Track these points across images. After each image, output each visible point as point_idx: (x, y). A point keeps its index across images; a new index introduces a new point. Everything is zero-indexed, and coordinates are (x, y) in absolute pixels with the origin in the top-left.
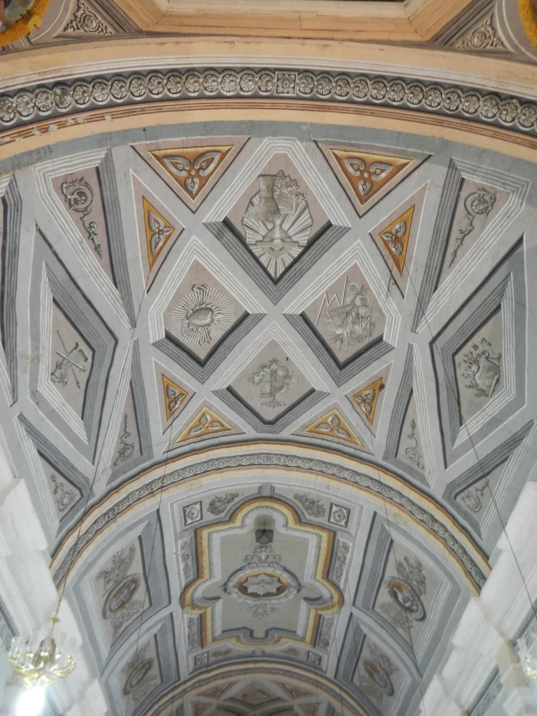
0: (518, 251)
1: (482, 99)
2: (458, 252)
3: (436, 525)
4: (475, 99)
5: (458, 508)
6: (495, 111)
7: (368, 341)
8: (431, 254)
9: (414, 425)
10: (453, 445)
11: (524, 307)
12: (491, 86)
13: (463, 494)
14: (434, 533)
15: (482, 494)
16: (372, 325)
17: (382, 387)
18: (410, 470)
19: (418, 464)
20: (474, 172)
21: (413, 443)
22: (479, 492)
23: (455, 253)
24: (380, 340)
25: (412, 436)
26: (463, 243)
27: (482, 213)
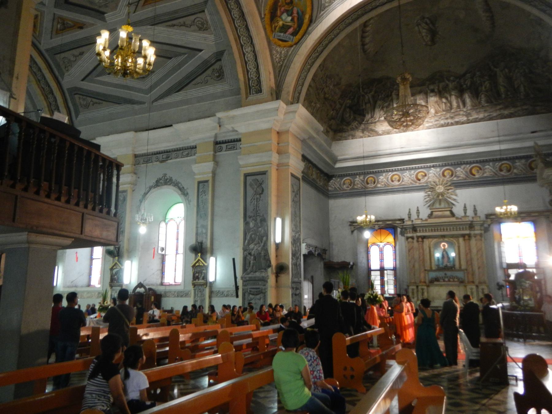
0: (197, 52)
1: (238, 9)
2: (176, 27)
3: (51, 95)
4: (237, 6)
5: (73, 99)
6: (238, 17)
7: (96, 7)
8: (164, 14)
9: (82, 54)
10: (96, 77)
11: (180, 68)
12: (245, 10)
13: (81, 96)
14: (46, 98)
15: (93, 104)
16: (106, 6)
17: (81, 28)
18: (58, 66)
19: (66, 67)
20: (210, 14)
21: (72, 59)
22: (92, 103)
23: (174, 25)
24: (104, 13)
25: (76, 57)
26: (181, 27)
27: (198, 27)
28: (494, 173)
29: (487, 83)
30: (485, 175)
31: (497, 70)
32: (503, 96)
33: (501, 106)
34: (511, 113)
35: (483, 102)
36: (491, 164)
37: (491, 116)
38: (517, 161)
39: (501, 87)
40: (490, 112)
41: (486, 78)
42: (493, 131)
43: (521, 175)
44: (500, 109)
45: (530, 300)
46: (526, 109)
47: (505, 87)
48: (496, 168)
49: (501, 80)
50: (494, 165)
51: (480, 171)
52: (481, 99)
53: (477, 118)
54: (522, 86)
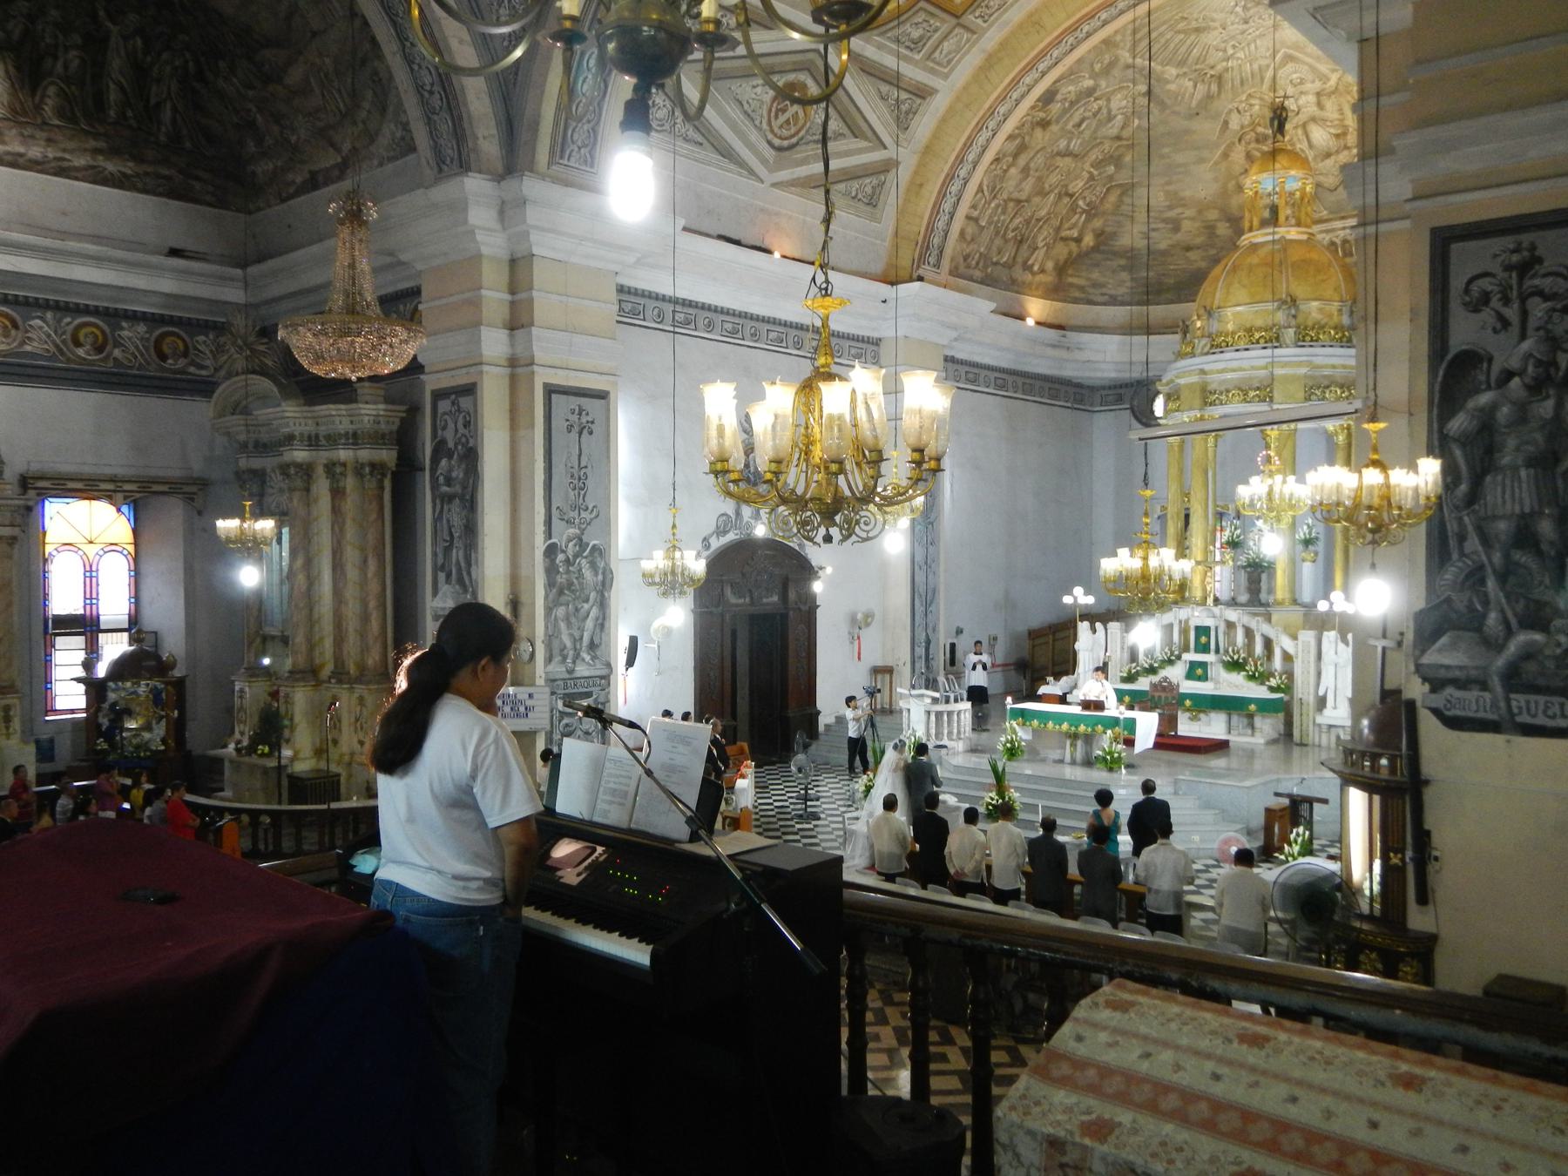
28: (57, 346)
29: (73, 53)
30: (28, 348)
31: (114, 29)
32: (112, 113)
33: (101, 144)
34: (124, 175)
35: (48, 109)
36: (49, 315)
37: (65, 164)
38: (124, 324)
39: (112, 86)
40: (64, 150)
41: (77, 39)
42: (64, 214)
43: (131, 368)
44: (96, 151)
45: (148, 727)
46: (164, 177)
47: (122, 89)
48: (64, 333)
49: (116, 64)
50: (59, 321)
51: (13, 332)
52: (43, 96)
53: (21, 155)
54: (169, 105)
